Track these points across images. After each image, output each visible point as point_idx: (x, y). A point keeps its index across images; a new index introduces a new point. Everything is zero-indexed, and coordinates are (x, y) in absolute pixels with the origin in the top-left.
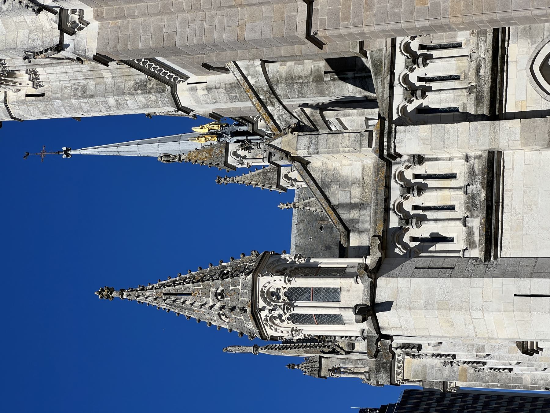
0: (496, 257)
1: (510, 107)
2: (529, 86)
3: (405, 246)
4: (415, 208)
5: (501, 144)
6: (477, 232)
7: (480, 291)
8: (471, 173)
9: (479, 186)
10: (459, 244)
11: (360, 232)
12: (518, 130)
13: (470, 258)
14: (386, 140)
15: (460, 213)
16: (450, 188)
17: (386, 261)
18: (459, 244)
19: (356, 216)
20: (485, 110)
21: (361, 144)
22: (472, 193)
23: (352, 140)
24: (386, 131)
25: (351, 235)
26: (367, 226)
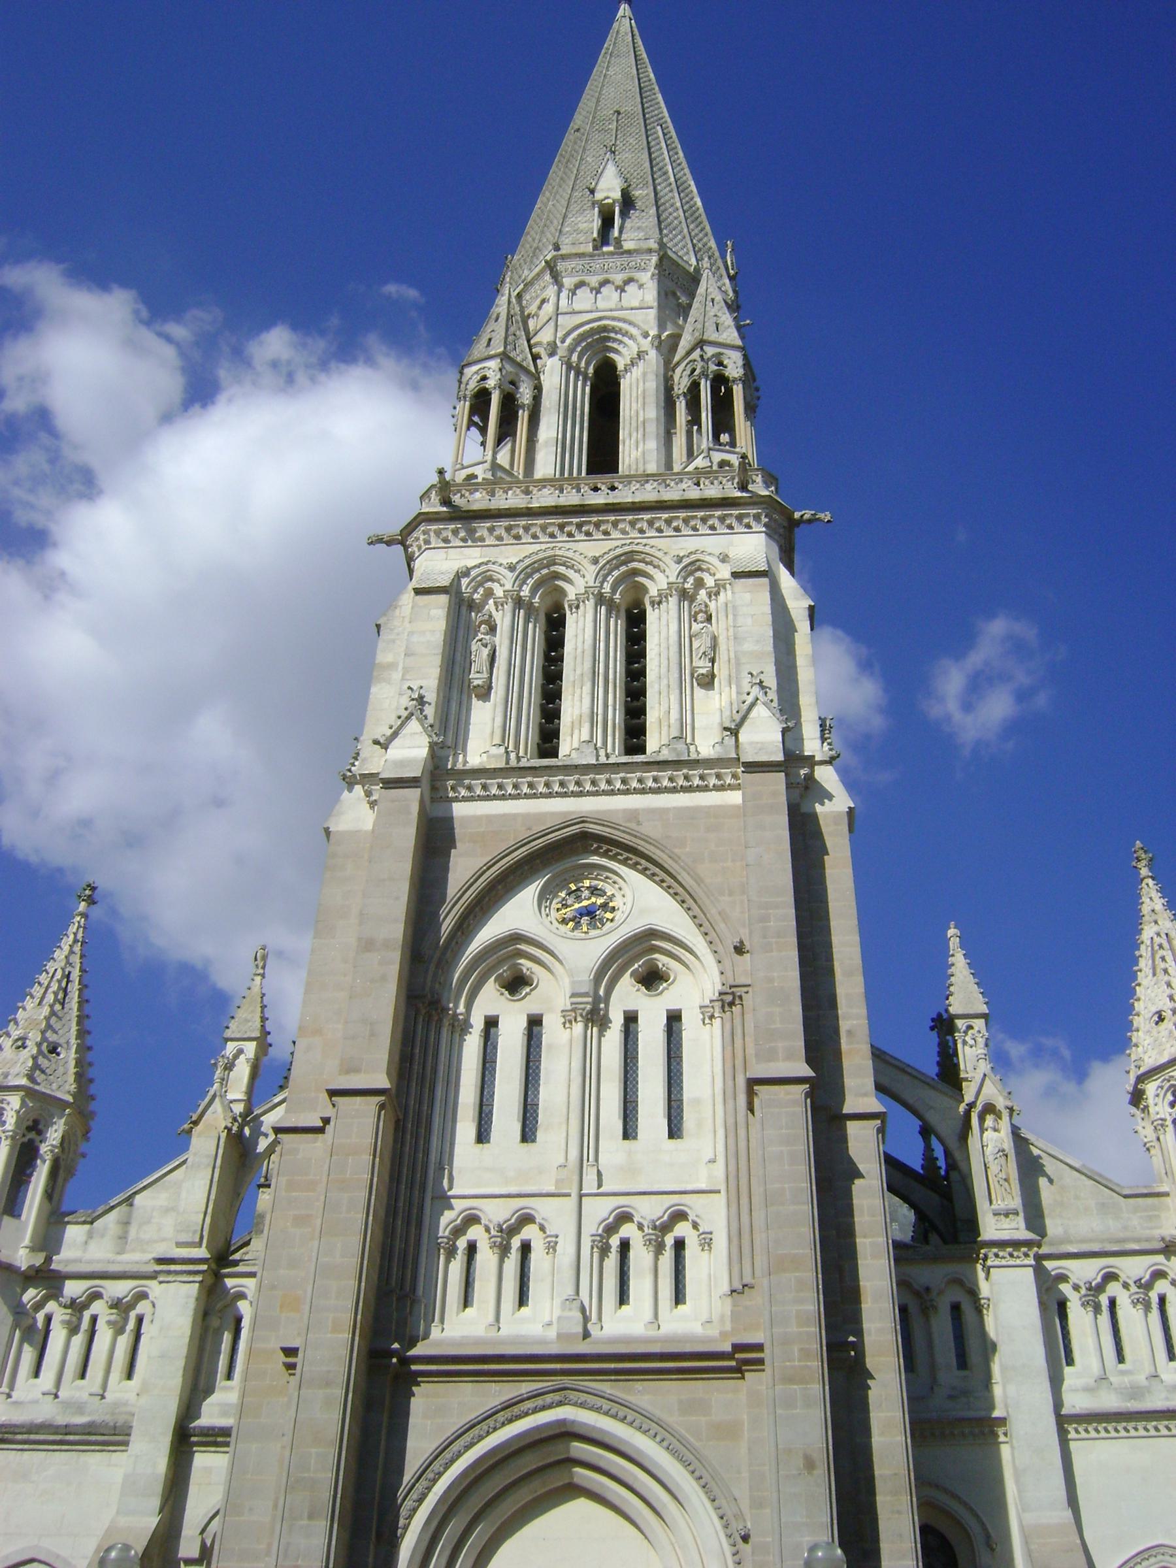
3: (39, 1306)
4: (94, 1319)
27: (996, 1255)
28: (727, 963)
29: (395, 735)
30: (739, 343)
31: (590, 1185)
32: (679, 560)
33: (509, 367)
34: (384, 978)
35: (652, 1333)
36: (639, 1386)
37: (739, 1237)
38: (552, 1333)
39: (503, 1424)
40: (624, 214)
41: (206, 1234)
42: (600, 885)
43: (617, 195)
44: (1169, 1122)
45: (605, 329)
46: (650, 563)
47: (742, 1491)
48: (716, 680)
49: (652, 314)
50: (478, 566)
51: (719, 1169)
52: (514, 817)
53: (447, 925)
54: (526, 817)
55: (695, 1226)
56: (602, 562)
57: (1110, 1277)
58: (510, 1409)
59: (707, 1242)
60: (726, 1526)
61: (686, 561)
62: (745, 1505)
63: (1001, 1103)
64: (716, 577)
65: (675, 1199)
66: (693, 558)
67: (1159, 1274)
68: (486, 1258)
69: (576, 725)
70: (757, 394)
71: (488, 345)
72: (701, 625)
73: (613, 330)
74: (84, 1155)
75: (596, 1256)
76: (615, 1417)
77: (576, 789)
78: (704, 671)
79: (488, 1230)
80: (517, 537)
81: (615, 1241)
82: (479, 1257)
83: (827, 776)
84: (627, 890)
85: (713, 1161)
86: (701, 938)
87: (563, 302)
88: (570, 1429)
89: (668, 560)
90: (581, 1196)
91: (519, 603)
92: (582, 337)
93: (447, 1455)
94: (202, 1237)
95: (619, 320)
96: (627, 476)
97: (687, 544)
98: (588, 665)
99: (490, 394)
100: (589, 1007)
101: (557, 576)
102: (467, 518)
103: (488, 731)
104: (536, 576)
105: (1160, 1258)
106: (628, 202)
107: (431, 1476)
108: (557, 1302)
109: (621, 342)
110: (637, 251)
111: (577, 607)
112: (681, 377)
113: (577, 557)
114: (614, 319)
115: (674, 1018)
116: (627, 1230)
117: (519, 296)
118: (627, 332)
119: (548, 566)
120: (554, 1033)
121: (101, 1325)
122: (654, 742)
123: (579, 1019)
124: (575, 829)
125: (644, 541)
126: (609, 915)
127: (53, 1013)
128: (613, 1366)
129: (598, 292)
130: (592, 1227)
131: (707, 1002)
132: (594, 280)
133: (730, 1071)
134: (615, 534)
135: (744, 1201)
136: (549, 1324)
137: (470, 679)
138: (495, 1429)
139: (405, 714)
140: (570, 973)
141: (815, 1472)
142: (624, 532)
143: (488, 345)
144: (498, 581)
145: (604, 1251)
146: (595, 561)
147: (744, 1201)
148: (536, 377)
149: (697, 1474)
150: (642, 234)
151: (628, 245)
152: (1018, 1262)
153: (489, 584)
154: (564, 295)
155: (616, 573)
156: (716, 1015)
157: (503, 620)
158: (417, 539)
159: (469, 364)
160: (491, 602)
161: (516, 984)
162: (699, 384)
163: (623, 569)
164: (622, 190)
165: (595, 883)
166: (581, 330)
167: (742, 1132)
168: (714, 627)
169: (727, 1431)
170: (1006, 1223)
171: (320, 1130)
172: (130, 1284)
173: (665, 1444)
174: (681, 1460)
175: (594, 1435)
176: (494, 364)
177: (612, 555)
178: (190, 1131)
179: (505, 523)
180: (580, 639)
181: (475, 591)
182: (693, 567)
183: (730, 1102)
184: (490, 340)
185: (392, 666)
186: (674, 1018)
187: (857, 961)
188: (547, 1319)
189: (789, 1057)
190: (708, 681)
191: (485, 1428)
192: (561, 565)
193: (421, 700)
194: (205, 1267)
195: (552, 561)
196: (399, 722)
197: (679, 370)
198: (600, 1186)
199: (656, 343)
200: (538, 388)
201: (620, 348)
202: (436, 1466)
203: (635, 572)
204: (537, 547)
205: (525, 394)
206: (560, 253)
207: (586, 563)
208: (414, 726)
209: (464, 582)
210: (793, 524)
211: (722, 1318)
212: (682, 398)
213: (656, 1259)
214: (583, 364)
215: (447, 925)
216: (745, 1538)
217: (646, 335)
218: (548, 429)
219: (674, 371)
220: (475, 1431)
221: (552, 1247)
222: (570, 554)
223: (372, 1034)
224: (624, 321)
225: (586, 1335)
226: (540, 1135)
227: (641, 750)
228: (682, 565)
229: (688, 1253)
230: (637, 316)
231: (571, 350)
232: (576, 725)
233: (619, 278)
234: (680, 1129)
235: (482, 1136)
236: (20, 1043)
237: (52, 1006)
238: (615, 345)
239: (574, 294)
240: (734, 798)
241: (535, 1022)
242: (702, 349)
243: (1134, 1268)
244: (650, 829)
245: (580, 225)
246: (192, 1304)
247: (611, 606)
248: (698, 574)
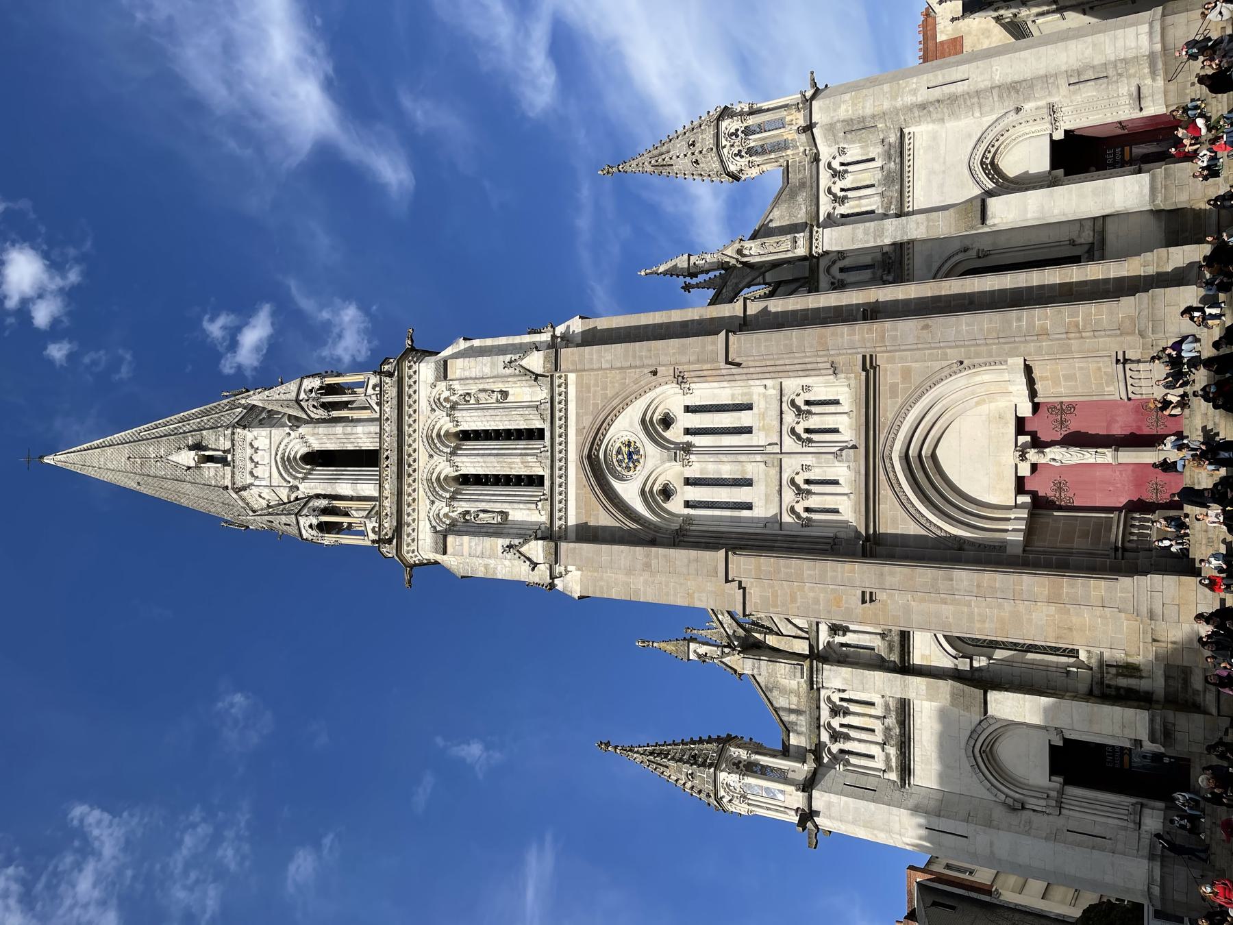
0: (909, 784)
1: (917, 659)
2: (932, 643)
4: (842, 725)
5: (911, 695)
6: (894, 760)
7: (897, 818)
8: (887, 706)
9: (895, 721)
10: (879, 763)
11: (798, 733)
12: (924, 687)
13: (889, 780)
14: (815, 676)
15: (879, 737)
16: (871, 716)
17: (821, 771)
18: (879, 763)
19: (795, 720)
20: (894, 657)
21: (795, 676)
22: (889, 726)
23: (787, 669)
24: (815, 669)
25: (791, 734)
26: (804, 729)
27: (817, 247)
28: (661, 380)
29: (529, 559)
30: (298, 380)
31: (776, 449)
32: (433, 410)
33: (305, 512)
34: (665, 556)
35: (853, 415)
36: (882, 420)
37: (806, 372)
38: (852, 465)
39: (902, 488)
40: (206, 448)
41: (796, 663)
43: (193, 453)
44: (751, 159)
45: (282, 459)
47: (937, 365)
48: (504, 390)
49: (274, 431)
51: (769, 383)
52: (577, 495)
53: (634, 526)
54: (577, 488)
55: (798, 395)
56: (432, 453)
57: (829, 191)
58: (894, 485)
59: (806, 388)
60: (956, 373)
61: (434, 406)
62: (944, 363)
63: (737, 246)
64: (444, 389)
65: (784, 405)
66: (432, 403)
67: (829, 166)
68: (813, 502)
69: (527, 464)
70: (329, 373)
71: (289, 525)
72: (473, 398)
73: (283, 454)
74: (751, 739)
75: (813, 445)
76: (898, 431)
77: (563, 461)
78: (499, 396)
79: (798, 502)
80: (414, 500)
81: (805, 436)
82: (812, 506)
83: (560, 330)
84: (619, 435)
86: (647, 395)
87: (263, 483)
88: (903, 455)
89: (432, 417)
90: (781, 453)
91: (452, 498)
92: (287, 471)
93: (917, 516)
94: (798, 664)
95: (277, 451)
96: (380, 442)
97: (424, 405)
98: (492, 459)
99: (321, 522)
100: (682, 452)
101: (438, 479)
102: (398, 530)
103: (527, 512)
104: (437, 489)
105: (821, 164)
106: (197, 447)
107: (928, 524)
108: (837, 464)
110: (232, 440)
111: (457, 467)
113: (428, 467)
114: (276, 454)
115: (688, 409)
116: (800, 429)
117: (254, 511)
119: (432, 483)
120: (694, 472)
121: (847, 720)
122: (537, 424)
123: (688, 457)
125: (421, 430)
126: (633, 444)
127: (673, 759)
128: (872, 432)
129: (257, 463)
130: (798, 447)
132: (250, 466)
133: (720, 377)
134: (415, 446)
135: (788, 368)
136: (849, 467)
137: (497, 524)
138: (904, 492)
139: (518, 554)
140: (663, 462)
141: (930, 323)
142: (414, 441)
143: (289, 525)
145: (810, 441)
146: (431, 456)
147: (788, 368)
148: (310, 498)
149: (928, 388)
150: (221, 438)
151: (228, 445)
152: (821, 236)
153: (441, 516)
154: (257, 483)
155: (438, 445)
156: (688, 386)
157: (461, 507)
158: (411, 557)
159: (301, 535)
160: (450, 514)
161: (667, 493)
162: (323, 403)
163: (436, 441)
164: (190, 450)
165: (614, 452)
166: (283, 472)
167: (752, 370)
168: (473, 392)
169: (906, 374)
170: (800, 242)
171: (744, 589)
172: (822, 705)
173: (912, 405)
174: (920, 397)
175: (907, 441)
176: (302, 520)
177: (428, 447)
178: (740, 675)
179: (405, 507)
180: (477, 464)
181: (444, 523)
182: (437, 403)
183: (737, 377)
184: (285, 524)
185: (486, 566)
186: (688, 409)
187: (664, 313)
188: (846, 468)
189: (714, 343)
190: (505, 394)
191: (901, 494)
193: (510, 547)
194: (815, 662)
195: (429, 481)
196: (522, 557)
197: (313, 415)
198: (777, 444)
199: (294, 428)
200: (318, 496)
201: (295, 450)
202: (923, 521)
203: (438, 435)
204: (421, 490)
205: (323, 503)
206: (230, 486)
207: (432, 461)
208: (524, 549)
209: (439, 528)
210: (413, 349)
211: (848, 379)
212: (330, 413)
213: (815, 414)
214: (305, 471)
215: (634, 526)
216: (961, 363)
217: (289, 434)
218: (344, 489)
219: (313, 418)
220: (905, 502)
221: (807, 468)
222: (426, 471)
223: (697, 561)
224: (278, 447)
225: (854, 447)
226: (748, 477)
227: (541, 431)
228: (436, 408)
229: (812, 399)
230: (276, 440)
231: (296, 478)
232: (525, 464)
233: (249, 451)
234: (747, 404)
235: (749, 506)
236: (690, 777)
237: (669, 760)
238: (293, 453)
239: (257, 477)
240: (572, 377)
241: (688, 482)
242: (301, 401)
243: (825, 178)
244: (587, 421)
245: (211, 475)
246: (835, 668)
247: (457, 448)
248: (442, 400)
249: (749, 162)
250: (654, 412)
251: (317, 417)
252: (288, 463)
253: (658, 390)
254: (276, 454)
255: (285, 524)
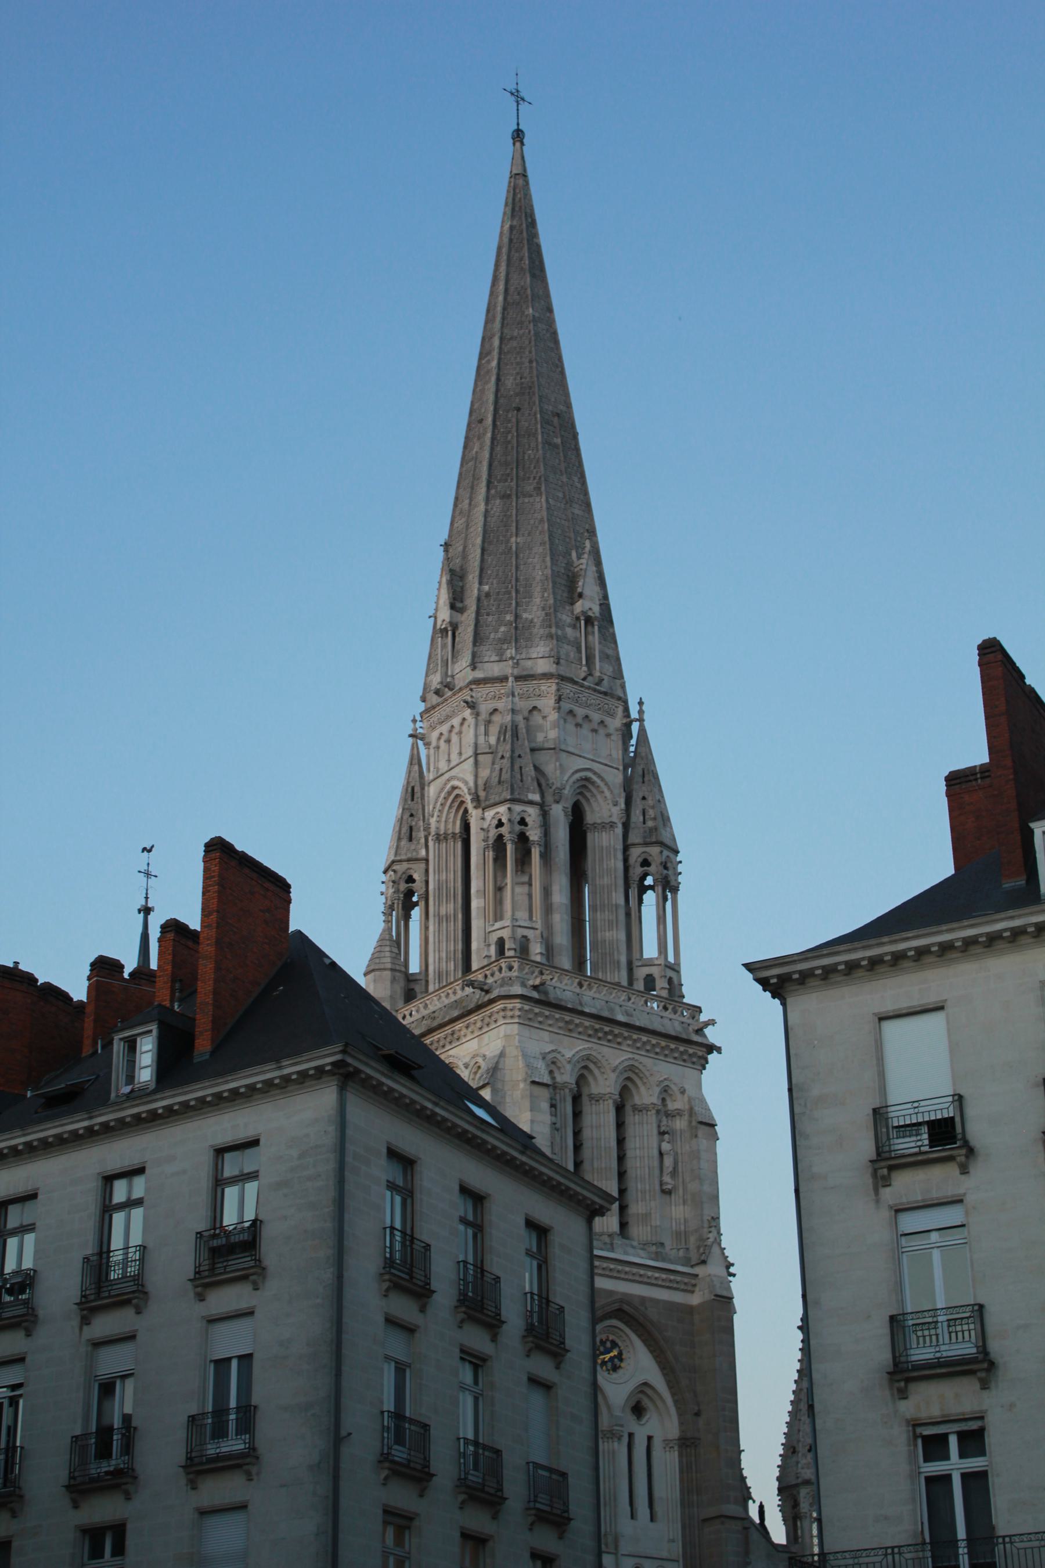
42: (618, 1341)
45: (587, 779)
46: (641, 1078)
50: (549, 1052)
71: (522, 781)
73: (593, 783)
85: (673, 1541)
101: (585, 1067)
109: (594, 796)
112: (636, 861)
114: (595, 773)
118: (603, 792)
124: (616, 1306)
131: (670, 1437)
144: (559, 1068)
184: (521, 768)
192: (592, 1062)
201: (592, 800)
203: (628, 1079)
222: (599, 1057)
224: (603, 780)
238: (588, 794)
242: (661, 852)
249: (806, 1513)
250: (648, 1396)
251: (632, 860)
252: (585, 785)
253: (673, 1410)
254: (595, 773)
255: (521, 768)
